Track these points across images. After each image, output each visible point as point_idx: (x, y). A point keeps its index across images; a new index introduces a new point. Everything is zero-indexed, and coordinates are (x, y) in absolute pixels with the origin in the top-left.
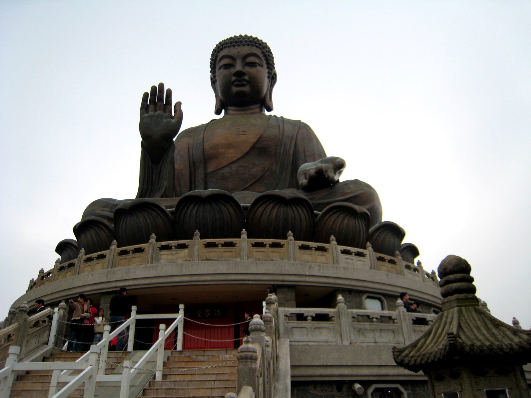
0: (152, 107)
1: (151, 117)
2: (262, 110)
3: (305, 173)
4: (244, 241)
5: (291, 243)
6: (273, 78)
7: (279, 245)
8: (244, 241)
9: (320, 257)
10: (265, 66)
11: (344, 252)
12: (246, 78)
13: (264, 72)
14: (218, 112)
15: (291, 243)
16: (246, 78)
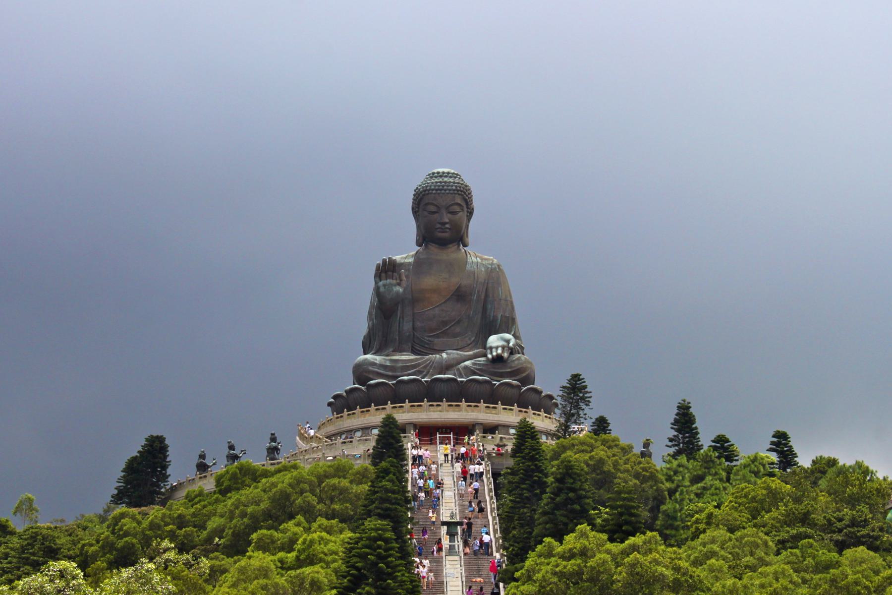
0: (383, 275)
1: (384, 285)
2: (459, 246)
3: (491, 348)
4: (463, 404)
5: (482, 405)
6: (470, 213)
7: (477, 406)
8: (463, 404)
9: (494, 411)
10: (465, 206)
11: (504, 409)
12: (447, 226)
13: (463, 215)
14: (419, 244)
15: (482, 405)
16: (447, 226)
